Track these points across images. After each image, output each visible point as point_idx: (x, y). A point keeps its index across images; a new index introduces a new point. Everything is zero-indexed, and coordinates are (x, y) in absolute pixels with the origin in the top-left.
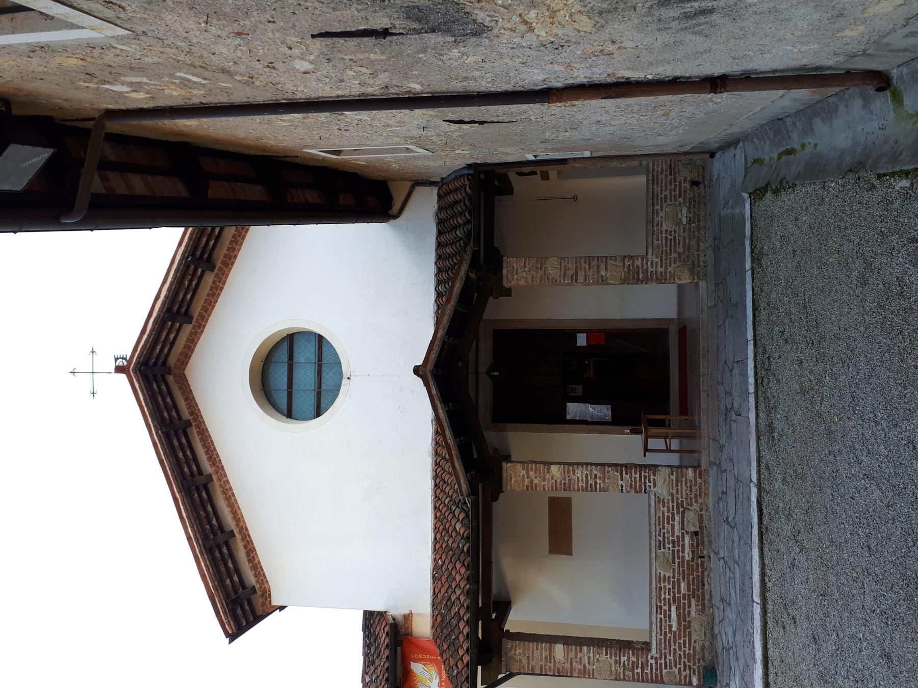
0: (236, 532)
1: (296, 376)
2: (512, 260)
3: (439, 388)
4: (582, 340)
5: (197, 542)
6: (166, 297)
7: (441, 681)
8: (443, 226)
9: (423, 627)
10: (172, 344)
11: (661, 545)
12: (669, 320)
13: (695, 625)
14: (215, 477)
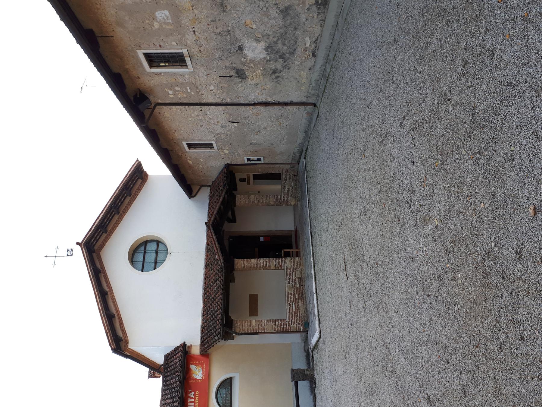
0: (116, 315)
1: (148, 253)
2: (239, 196)
3: (214, 230)
4: (262, 239)
5: (103, 311)
6: (102, 218)
7: (203, 372)
8: (211, 198)
9: (196, 351)
10: (97, 241)
11: (289, 283)
12: (292, 231)
13: (301, 309)
14: (109, 293)
